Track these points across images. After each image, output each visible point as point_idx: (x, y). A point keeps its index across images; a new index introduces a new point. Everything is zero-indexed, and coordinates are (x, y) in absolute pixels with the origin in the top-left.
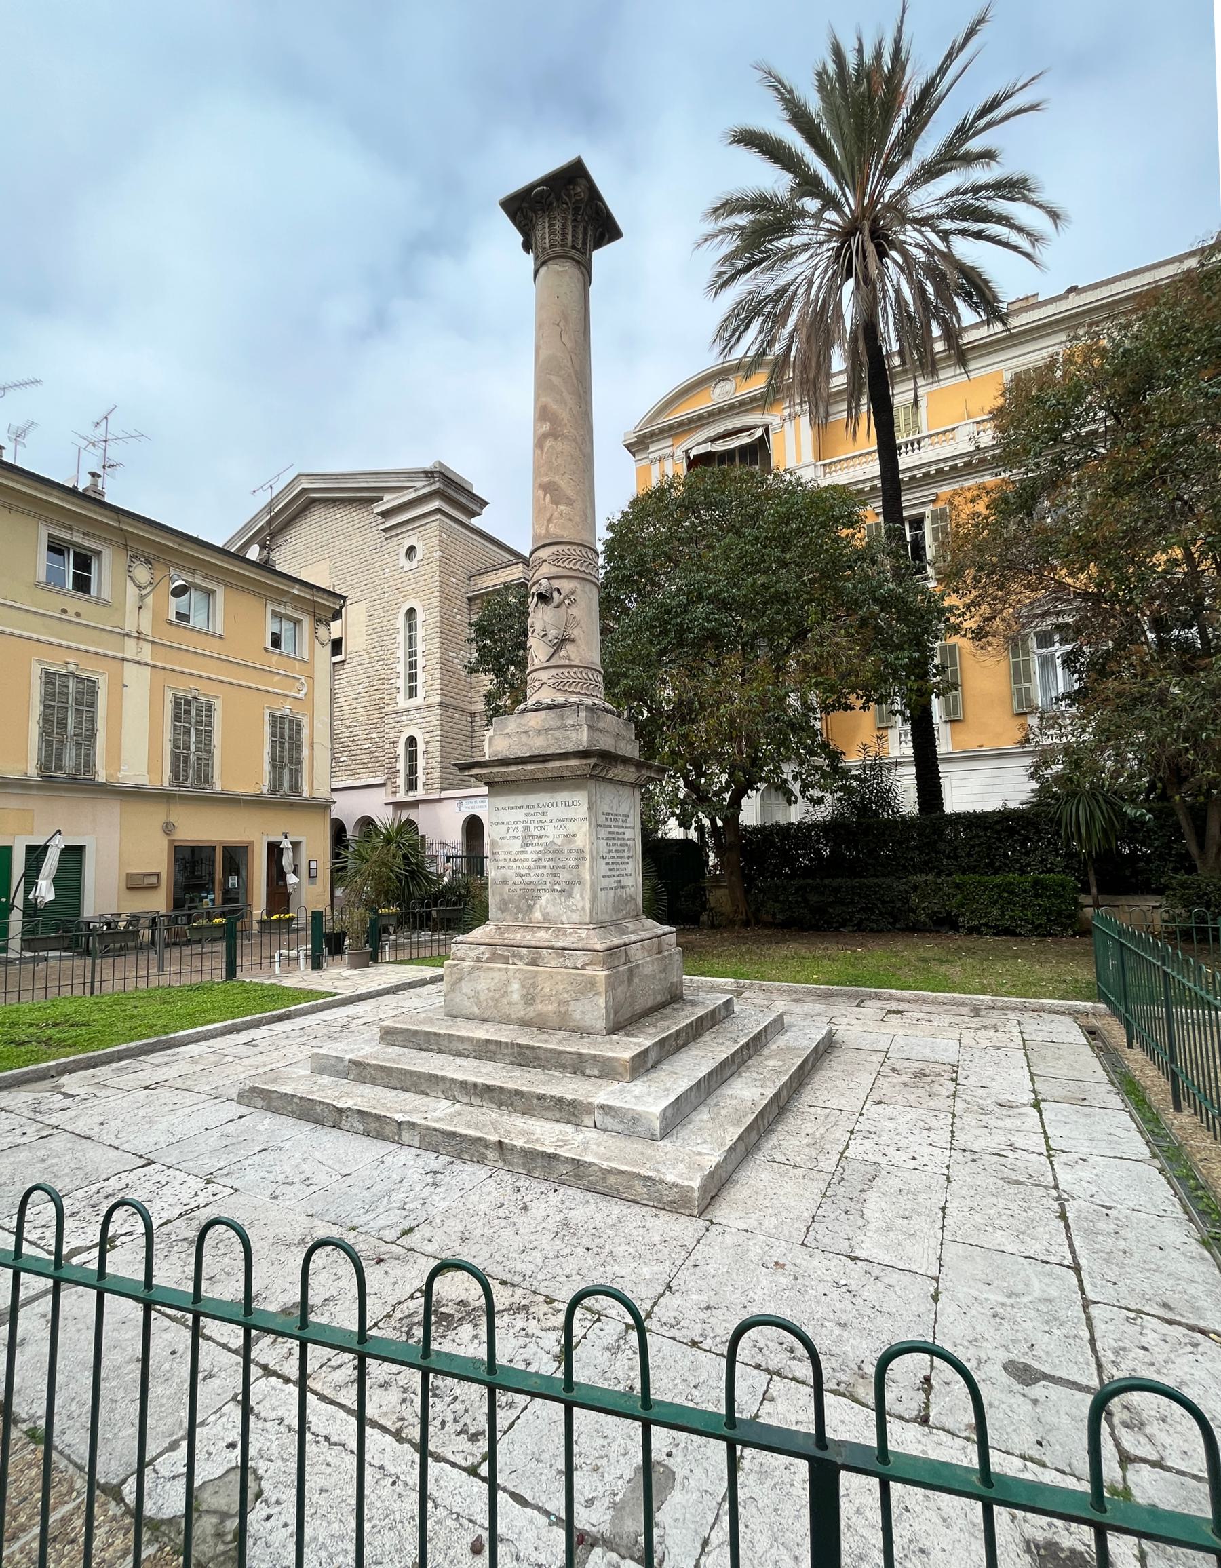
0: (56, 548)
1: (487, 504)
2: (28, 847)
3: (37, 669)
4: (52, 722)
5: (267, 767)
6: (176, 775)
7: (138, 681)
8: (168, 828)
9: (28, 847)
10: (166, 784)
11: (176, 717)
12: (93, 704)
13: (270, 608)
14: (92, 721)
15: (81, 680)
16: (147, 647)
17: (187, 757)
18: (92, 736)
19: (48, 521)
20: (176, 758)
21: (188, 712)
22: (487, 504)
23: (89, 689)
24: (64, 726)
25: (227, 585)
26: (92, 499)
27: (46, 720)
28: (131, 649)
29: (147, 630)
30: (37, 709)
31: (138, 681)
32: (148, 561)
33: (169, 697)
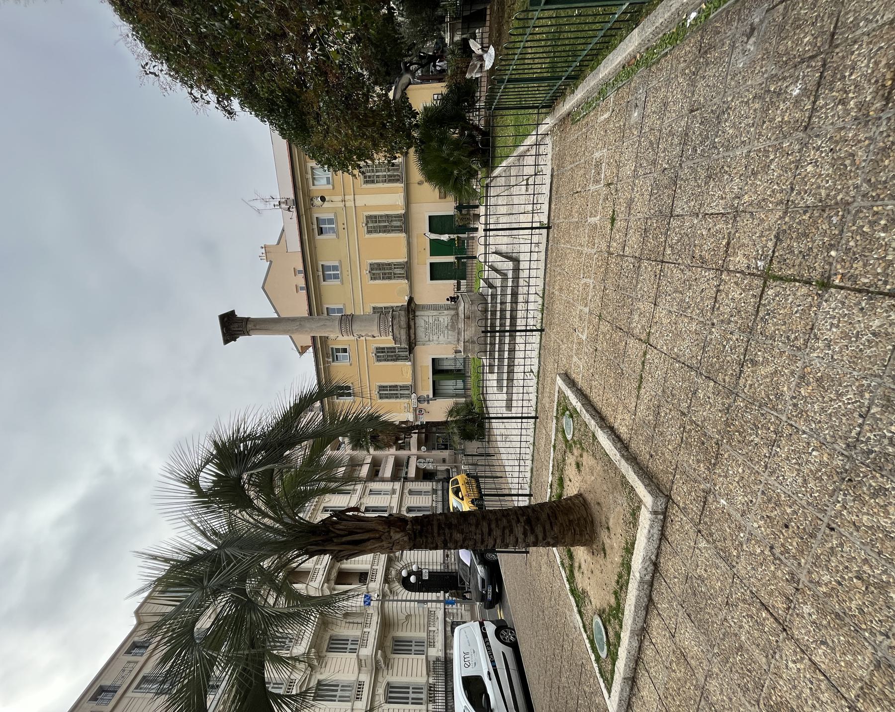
0: (321, 231)
1: (226, 341)
2: (432, 278)
3: (367, 236)
4: (385, 230)
5: (389, 235)
6: (397, 181)
7: (361, 200)
8: (420, 183)
9: (432, 278)
10: (402, 185)
11: (373, 182)
12: (375, 217)
13: (318, 237)
14: (381, 216)
15: (367, 222)
16: (347, 197)
17: (389, 176)
18: (387, 216)
19: (314, 238)
20: (390, 181)
21: (370, 177)
22: (226, 341)
23: (369, 218)
24: (386, 226)
25: (317, 263)
26: (296, 202)
27: (384, 232)
28: (350, 204)
29: (340, 198)
30: (381, 235)
31: (361, 200)
32: (312, 200)
33: (364, 186)
